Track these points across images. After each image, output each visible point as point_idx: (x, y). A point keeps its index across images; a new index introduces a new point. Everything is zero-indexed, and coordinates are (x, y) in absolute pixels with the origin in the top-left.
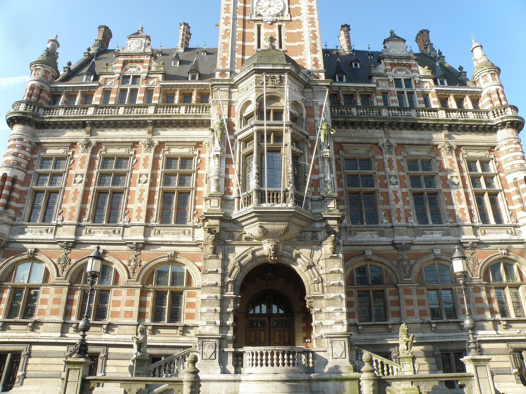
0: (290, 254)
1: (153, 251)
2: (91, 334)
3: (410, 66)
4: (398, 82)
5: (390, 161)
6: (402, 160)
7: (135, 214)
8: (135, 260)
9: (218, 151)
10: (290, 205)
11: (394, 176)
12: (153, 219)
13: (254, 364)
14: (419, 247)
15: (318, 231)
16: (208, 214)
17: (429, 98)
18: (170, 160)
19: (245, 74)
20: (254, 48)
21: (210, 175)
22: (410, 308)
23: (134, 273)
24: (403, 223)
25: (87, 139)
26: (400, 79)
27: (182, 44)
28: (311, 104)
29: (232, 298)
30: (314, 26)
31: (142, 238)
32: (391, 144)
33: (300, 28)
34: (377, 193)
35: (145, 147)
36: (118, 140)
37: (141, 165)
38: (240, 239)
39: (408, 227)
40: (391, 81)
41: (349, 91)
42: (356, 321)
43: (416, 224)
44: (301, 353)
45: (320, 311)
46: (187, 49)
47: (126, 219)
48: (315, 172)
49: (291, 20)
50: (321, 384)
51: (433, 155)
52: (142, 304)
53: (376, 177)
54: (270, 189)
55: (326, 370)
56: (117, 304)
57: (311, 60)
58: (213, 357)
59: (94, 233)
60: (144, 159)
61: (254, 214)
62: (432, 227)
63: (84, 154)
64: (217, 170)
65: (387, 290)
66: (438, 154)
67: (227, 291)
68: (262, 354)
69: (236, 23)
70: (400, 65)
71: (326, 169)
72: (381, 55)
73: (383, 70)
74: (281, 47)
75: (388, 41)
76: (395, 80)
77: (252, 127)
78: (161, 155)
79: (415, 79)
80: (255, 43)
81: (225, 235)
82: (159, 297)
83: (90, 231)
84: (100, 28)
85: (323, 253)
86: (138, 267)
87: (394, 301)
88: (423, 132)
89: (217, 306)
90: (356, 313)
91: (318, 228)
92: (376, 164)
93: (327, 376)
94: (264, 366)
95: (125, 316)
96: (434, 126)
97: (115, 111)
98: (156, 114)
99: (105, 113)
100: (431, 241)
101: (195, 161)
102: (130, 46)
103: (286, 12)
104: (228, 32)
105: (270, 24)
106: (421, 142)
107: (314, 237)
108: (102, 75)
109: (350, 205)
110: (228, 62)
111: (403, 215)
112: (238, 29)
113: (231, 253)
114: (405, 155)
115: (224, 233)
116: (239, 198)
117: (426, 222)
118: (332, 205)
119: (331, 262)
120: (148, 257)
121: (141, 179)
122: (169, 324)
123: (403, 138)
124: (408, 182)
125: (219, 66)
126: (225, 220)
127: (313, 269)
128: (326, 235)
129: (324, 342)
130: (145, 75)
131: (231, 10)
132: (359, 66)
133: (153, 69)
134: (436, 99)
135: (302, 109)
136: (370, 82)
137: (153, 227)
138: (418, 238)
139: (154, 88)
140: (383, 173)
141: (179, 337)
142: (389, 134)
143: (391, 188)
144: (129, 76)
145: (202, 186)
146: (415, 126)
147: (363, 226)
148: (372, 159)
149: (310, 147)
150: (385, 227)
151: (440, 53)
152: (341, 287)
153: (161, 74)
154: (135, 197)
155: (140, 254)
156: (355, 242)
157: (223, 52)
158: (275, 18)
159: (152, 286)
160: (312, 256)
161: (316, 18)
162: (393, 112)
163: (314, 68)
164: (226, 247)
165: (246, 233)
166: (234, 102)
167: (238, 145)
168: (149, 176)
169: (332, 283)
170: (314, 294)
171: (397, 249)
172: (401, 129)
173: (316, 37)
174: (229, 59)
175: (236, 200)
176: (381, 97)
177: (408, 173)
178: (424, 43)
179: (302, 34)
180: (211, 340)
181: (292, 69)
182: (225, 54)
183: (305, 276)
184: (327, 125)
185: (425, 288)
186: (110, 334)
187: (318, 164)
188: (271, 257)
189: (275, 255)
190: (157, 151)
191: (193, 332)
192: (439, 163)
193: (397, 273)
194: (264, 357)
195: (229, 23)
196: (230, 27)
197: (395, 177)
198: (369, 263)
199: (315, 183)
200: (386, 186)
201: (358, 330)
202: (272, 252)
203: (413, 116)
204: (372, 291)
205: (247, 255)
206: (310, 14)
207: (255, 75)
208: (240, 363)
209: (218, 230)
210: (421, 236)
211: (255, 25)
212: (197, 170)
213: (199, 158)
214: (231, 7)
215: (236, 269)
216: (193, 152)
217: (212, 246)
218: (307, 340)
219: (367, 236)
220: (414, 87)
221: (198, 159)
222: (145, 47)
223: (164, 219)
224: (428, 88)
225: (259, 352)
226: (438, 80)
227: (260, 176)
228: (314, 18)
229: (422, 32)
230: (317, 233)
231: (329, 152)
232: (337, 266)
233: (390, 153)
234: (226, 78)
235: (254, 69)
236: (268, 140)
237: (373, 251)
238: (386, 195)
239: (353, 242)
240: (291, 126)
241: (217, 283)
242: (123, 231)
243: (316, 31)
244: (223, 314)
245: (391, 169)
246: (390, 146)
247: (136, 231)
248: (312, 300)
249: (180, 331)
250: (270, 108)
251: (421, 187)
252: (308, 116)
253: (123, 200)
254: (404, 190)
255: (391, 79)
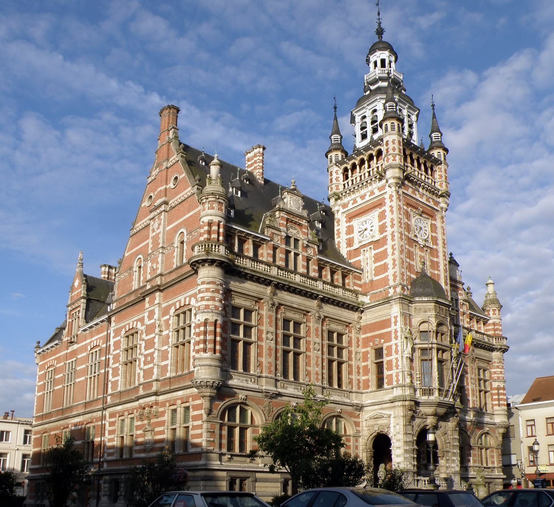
36: (295, 306)
63: (271, 313)
144: (291, 237)
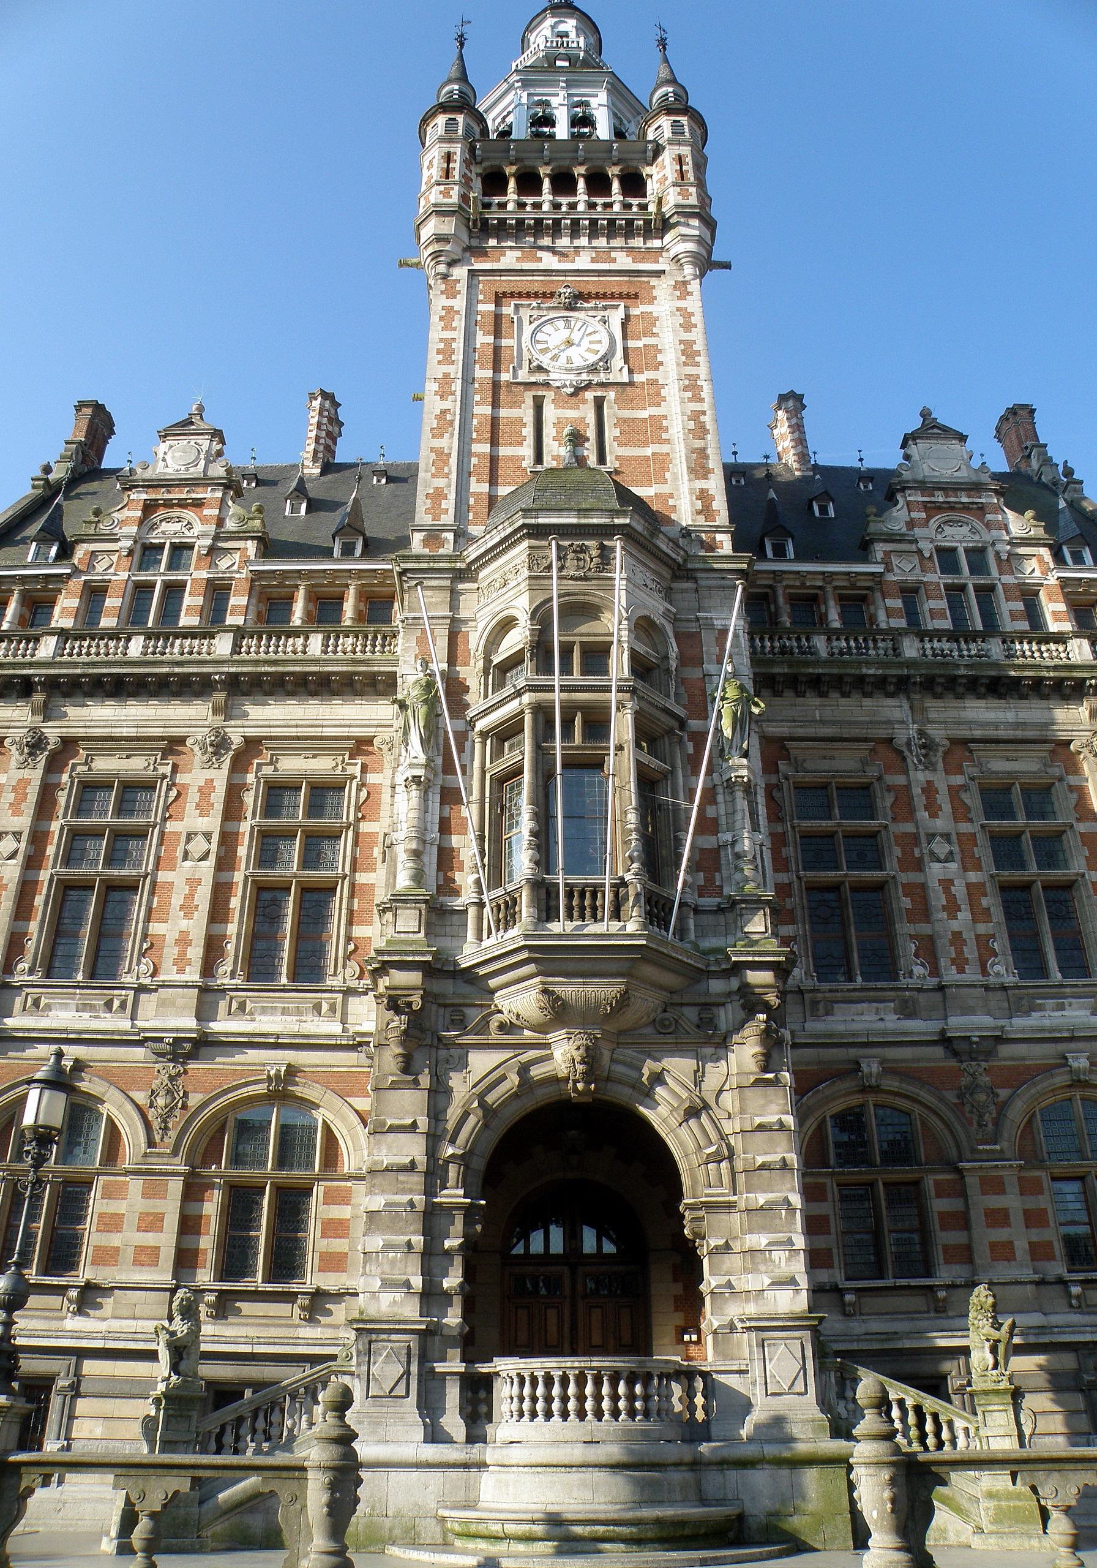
0: (633, 1074)
1: (222, 1062)
2: (32, 1317)
3: (982, 509)
4: (947, 558)
5: (929, 789)
6: (965, 788)
7: (171, 952)
8: (169, 1092)
9: (417, 766)
10: (632, 927)
11: (942, 835)
12: (226, 967)
13: (526, 1413)
14: (1021, 1049)
15: (718, 1005)
16: (389, 953)
17: (1040, 604)
18: (276, 793)
19: (497, 539)
20: (525, 464)
21: (395, 836)
22: (1000, 1234)
23: (166, 1129)
24: (971, 975)
25: (33, 729)
26: (954, 550)
27: (315, 452)
28: (693, 627)
29: (458, 1207)
30: (697, 398)
31: (191, 1023)
32: (933, 741)
33: (659, 405)
34: (892, 886)
35: (205, 753)
36: (125, 732)
37: (190, 806)
38: (483, 1027)
39: (987, 988)
40: (927, 555)
41: (803, 585)
42: (835, 1275)
43: (1011, 980)
44: (669, 1377)
45: (727, 1246)
46: (328, 468)
47: (143, 968)
48: (707, 825)
49: (631, 383)
50: (732, 1475)
51: (1056, 771)
52: (189, 1225)
53: (888, 839)
54: (574, 879)
55: (745, 1432)
56: (112, 1223)
57: (690, 498)
58: (401, 1390)
59: (48, 1007)
60: (200, 789)
61: (525, 955)
62: (1061, 986)
63: (26, 773)
64: (415, 822)
65: (930, 1181)
66: (1072, 765)
67: (444, 1187)
68: (549, 1381)
69: (471, 391)
70: (951, 507)
71: (739, 816)
72: (895, 480)
73: (902, 524)
74: (602, 459)
75: (914, 439)
76: (940, 550)
77: (519, 693)
78: (250, 778)
79: (999, 547)
80: (527, 451)
81: (438, 1016)
82: (241, 1202)
83: (36, 1003)
84: (79, 407)
85: (734, 1070)
86: (177, 1112)
87: (952, 1215)
88: (1024, 703)
89: (414, 1233)
90: (835, 1251)
91: (719, 995)
92: (889, 800)
93: (751, 1451)
94: (556, 1418)
95: (137, 1263)
96: (1059, 683)
97: (117, 648)
98: (236, 657)
99: (88, 654)
100: (1060, 1031)
101: (351, 796)
102: (164, 460)
103: (618, 361)
104: (449, 417)
105: (572, 395)
106: (1019, 734)
107: (707, 1022)
108: (83, 541)
109: (812, 923)
110: (449, 504)
111: (970, 952)
112: (477, 410)
113: (454, 1070)
114: (974, 771)
115: (438, 1011)
116: (481, 905)
117: (1043, 971)
118: (758, 925)
119: (755, 1097)
120: (209, 1082)
121: (189, 847)
122: (270, 1287)
123: (965, 723)
124: (983, 851)
125: (423, 517)
126: (440, 970)
127: (704, 1118)
128: (742, 1015)
129: (739, 1345)
130: (208, 542)
131: (458, 357)
132: (832, 513)
133: (231, 525)
134: (1062, 607)
135: (666, 642)
136: (865, 560)
137: (224, 990)
138: (1019, 1022)
139: (231, 579)
140: (909, 828)
141: (298, 1326)
142: (924, 710)
143: (935, 871)
144: (161, 546)
145: (371, 868)
146: (1000, 686)
147: (851, 986)
148: (876, 785)
149: (691, 751)
150: (920, 990)
151: (1069, 472)
152: (787, 1173)
153: (253, 538)
154: (173, 901)
155: (186, 1072)
156: (831, 1036)
157: (433, 476)
158: (584, 376)
159: (220, 1170)
160: (698, 1078)
161: (702, 377)
162: (936, 644)
163: (701, 520)
164: (443, 1053)
165: (501, 1012)
166: (465, 622)
167: (478, 746)
168: (215, 838)
169: (760, 1160)
170: (706, 1194)
171: (956, 1054)
172: (960, 697)
173: (706, 432)
174: (452, 496)
175: (472, 912)
176: (897, 603)
177: (982, 826)
178: (1020, 442)
179: (665, 423)
180: (394, 1337)
181: (635, 525)
182: (441, 482)
183: (681, 1141)
184: (742, 688)
185: (1043, 1175)
186: (88, 1315)
187: (714, 802)
188: (575, 1082)
189: (588, 1077)
190: (240, 764)
191: (339, 1312)
192: (1075, 795)
193: (959, 1128)
194: (556, 1390)
195: (453, 393)
196: (453, 404)
197: (947, 837)
198: (871, 1099)
199: (708, 861)
200: (918, 865)
201: (843, 1304)
202: (580, 1068)
203: (995, 657)
204: (884, 1184)
205: (503, 1078)
206: (685, 364)
207: (526, 543)
208: (484, 1409)
209: (417, 1001)
210: (1027, 1013)
211: (529, 397)
212: (358, 820)
213: (364, 785)
214: (459, 346)
215: (472, 1120)
216: (344, 770)
217: (399, 1050)
218: (686, 1338)
219: (864, 1018)
220: (995, 572)
221: (359, 790)
222: (208, 462)
223: (258, 967)
224: (1037, 574)
225: (539, 1374)
226: (1065, 549)
227: (542, 839)
228: (698, 377)
229: (1013, 411)
230: (715, 1009)
231: (748, 768)
232: (776, 1109)
233: (930, 766)
234: (441, 551)
235: (524, 526)
236: (567, 733)
237: (883, 1062)
238: (920, 892)
239: (825, 1036)
240: (633, 691)
241: (413, 1162)
242: (136, 1002)
243: (704, 413)
244: (432, 1258)
245: (934, 816)
246: (929, 746)
247: (173, 1004)
248: (702, 1213)
249: (302, 1308)
250: (571, 639)
251: (1023, 866)
252: (683, 660)
253: (138, 912)
254: (973, 877)
255: (927, 548)
